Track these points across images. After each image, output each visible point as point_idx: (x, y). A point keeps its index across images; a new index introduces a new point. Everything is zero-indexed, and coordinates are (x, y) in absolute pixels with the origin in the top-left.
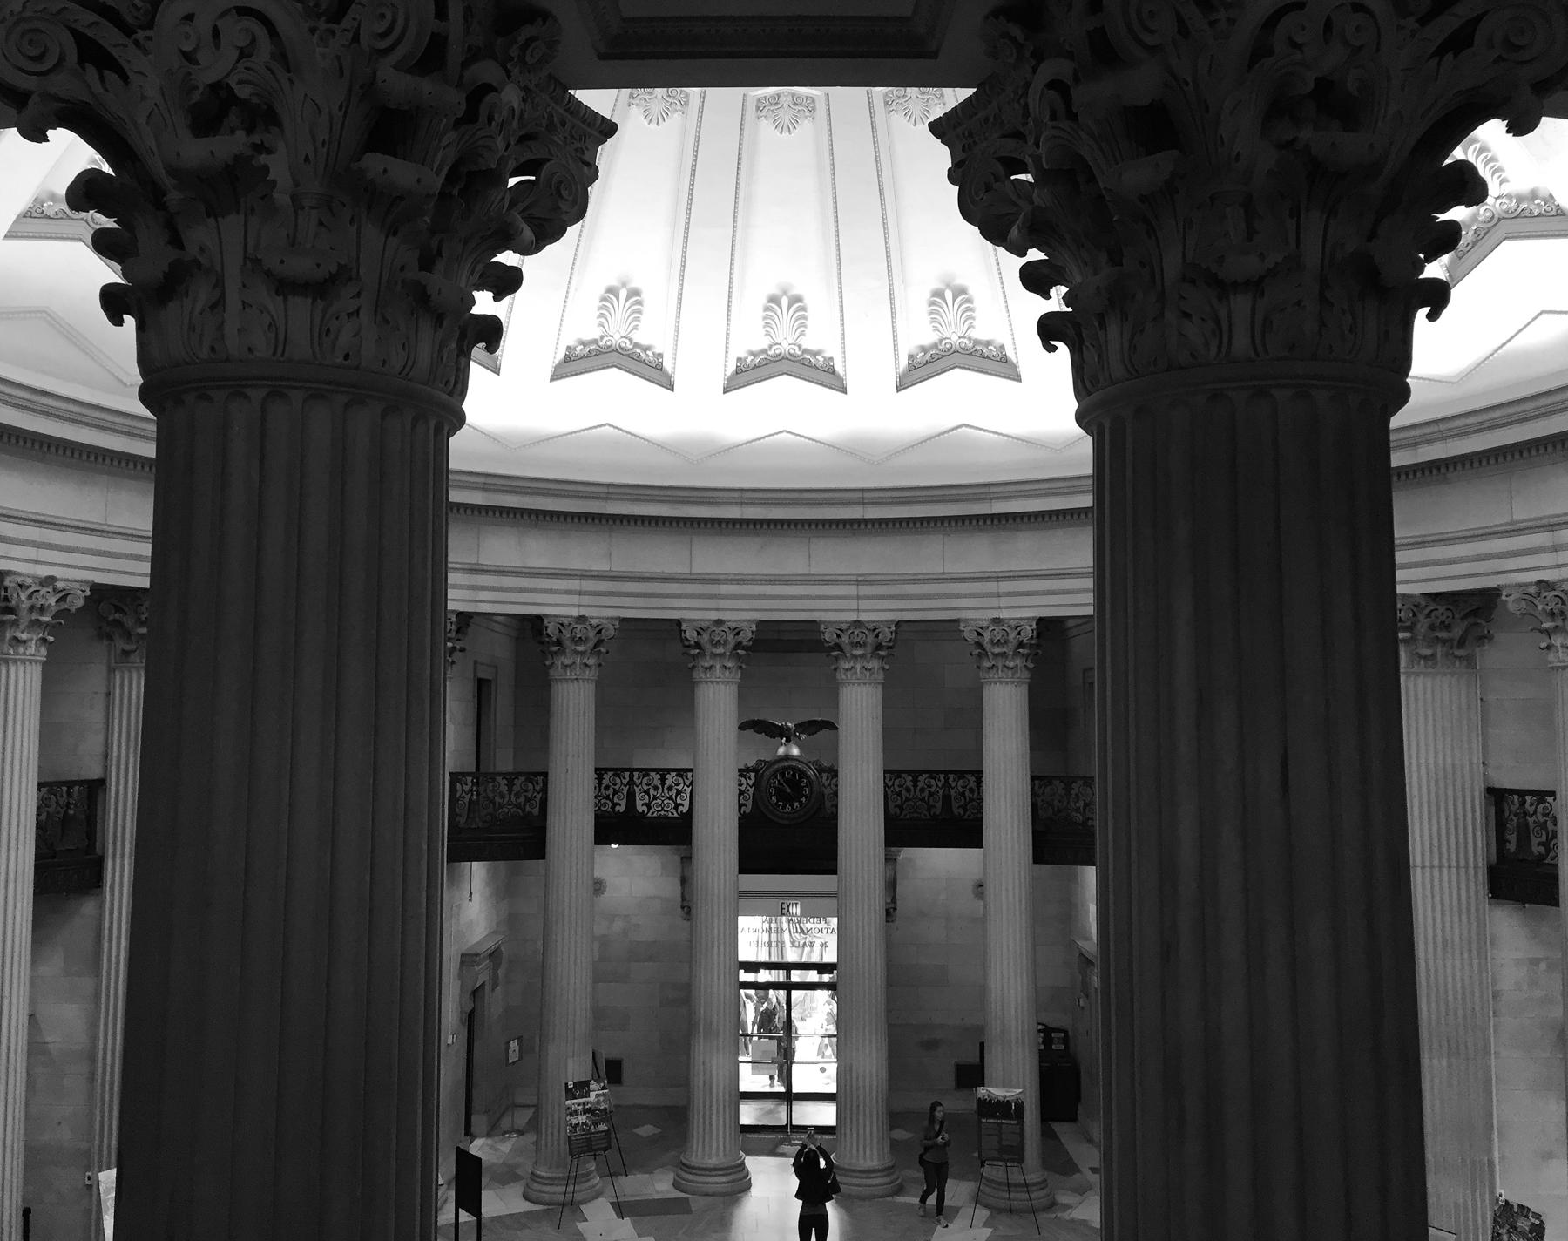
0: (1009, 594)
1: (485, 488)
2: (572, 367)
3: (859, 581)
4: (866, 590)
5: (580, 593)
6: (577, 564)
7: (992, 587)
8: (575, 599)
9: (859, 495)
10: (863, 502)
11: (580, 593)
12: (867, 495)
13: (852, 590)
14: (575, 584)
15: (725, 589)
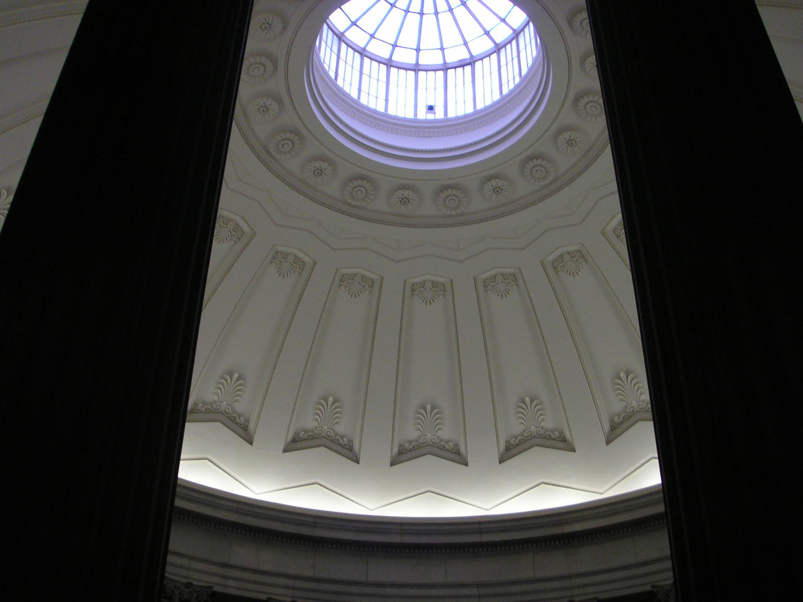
0: (579, 587)
1: (237, 511)
2: (299, 445)
3: (479, 585)
4: (483, 591)
5: (294, 588)
6: (293, 570)
7: (566, 583)
8: (290, 592)
9: (477, 526)
10: (480, 532)
11: (294, 588)
12: (483, 526)
13: (475, 591)
14: (290, 582)
15: (390, 591)
